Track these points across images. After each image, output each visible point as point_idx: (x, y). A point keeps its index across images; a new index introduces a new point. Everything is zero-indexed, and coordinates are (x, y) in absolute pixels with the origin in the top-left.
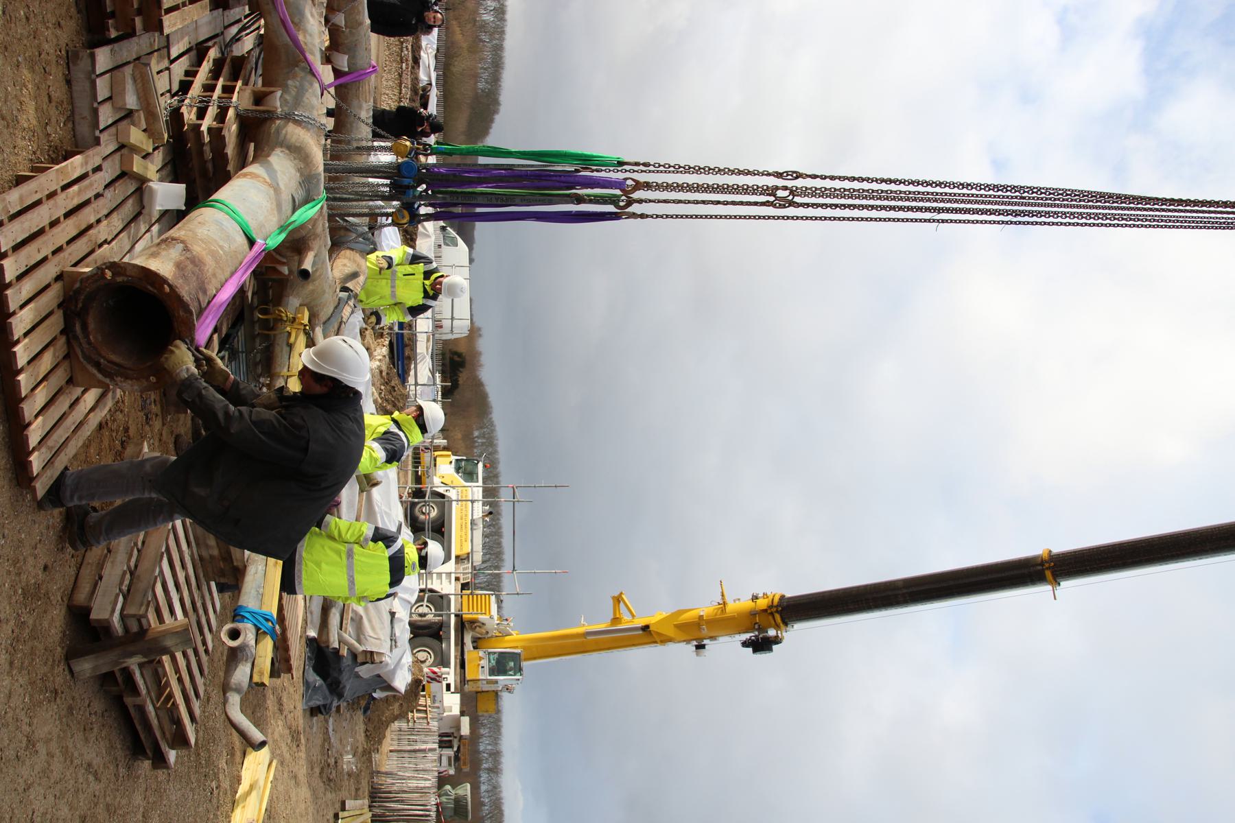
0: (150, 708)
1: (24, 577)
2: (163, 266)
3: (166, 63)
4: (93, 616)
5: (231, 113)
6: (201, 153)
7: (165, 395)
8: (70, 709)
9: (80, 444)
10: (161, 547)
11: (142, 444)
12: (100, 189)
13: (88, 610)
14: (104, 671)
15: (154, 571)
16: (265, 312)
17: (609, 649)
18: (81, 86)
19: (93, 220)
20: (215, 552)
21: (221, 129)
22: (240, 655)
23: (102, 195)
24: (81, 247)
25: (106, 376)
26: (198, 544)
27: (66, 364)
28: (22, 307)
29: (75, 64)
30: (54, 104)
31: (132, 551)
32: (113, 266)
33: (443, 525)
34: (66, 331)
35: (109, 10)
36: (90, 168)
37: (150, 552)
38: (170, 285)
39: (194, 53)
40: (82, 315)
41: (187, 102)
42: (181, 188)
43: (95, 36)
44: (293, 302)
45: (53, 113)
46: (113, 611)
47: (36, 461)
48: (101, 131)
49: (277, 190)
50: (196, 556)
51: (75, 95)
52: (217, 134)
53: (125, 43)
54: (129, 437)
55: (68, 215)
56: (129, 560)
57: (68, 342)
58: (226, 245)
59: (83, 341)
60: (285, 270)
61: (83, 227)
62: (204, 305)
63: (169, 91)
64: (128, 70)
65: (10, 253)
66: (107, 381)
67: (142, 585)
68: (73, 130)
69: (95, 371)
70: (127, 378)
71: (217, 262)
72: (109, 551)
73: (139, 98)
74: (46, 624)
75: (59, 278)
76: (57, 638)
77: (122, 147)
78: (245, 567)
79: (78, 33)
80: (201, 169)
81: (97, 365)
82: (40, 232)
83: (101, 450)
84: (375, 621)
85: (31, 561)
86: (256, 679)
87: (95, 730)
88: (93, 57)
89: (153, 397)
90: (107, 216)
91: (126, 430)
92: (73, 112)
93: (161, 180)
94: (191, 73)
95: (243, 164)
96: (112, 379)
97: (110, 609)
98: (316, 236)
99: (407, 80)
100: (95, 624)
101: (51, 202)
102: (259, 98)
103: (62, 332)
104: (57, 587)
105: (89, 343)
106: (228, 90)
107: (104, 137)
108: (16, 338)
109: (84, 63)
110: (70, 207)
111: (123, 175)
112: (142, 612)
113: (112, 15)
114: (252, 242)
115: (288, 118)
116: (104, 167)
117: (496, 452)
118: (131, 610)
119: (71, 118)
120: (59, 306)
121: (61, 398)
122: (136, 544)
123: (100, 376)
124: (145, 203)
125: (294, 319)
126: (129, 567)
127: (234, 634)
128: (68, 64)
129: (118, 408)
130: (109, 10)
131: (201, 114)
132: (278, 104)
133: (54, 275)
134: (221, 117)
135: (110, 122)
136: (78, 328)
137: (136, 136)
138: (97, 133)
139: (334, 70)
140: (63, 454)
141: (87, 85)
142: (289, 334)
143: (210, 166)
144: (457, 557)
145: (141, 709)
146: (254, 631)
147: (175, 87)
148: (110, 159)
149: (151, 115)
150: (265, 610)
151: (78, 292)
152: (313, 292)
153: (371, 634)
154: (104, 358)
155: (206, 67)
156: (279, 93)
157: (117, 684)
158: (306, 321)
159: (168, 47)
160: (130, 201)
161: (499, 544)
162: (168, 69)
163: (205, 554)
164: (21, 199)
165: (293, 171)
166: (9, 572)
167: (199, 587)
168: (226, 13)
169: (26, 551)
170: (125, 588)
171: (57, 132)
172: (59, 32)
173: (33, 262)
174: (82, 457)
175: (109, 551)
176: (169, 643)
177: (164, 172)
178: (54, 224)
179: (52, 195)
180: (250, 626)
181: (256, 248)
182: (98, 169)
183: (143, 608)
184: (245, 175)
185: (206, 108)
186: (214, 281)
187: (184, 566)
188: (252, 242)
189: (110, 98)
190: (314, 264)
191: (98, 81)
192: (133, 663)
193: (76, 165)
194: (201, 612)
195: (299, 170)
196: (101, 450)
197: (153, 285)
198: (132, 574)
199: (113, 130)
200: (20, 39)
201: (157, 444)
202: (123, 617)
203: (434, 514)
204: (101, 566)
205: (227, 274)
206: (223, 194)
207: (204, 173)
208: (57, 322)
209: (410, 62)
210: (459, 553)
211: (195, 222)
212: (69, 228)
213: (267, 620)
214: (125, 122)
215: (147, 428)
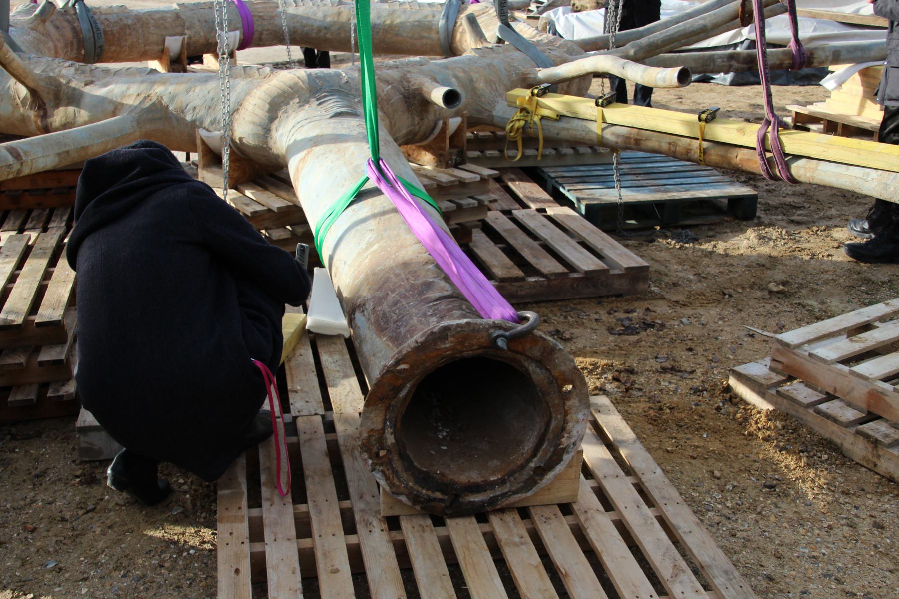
7: (619, 295)
25: (560, 460)
38: (397, 363)
44: (500, 110)
49: (316, 141)
59: (498, 491)
60: (454, 123)
62: (448, 290)
66: (567, 458)
69: (551, 475)
70: (563, 429)
75: (393, 523)
81: (541, 471)
89: (622, 315)
96: (565, 450)
98: (404, 79)
102: (213, 158)
105: (502, 482)
120: (438, 522)
121: (592, 535)
123: (559, 468)
125: (523, 110)
136: (477, 498)
142: (543, 118)
151: (415, 499)
154: (529, 461)
156: (202, 133)
158: (528, 92)
188: (360, 195)
197: (397, 390)
201: (689, 311)
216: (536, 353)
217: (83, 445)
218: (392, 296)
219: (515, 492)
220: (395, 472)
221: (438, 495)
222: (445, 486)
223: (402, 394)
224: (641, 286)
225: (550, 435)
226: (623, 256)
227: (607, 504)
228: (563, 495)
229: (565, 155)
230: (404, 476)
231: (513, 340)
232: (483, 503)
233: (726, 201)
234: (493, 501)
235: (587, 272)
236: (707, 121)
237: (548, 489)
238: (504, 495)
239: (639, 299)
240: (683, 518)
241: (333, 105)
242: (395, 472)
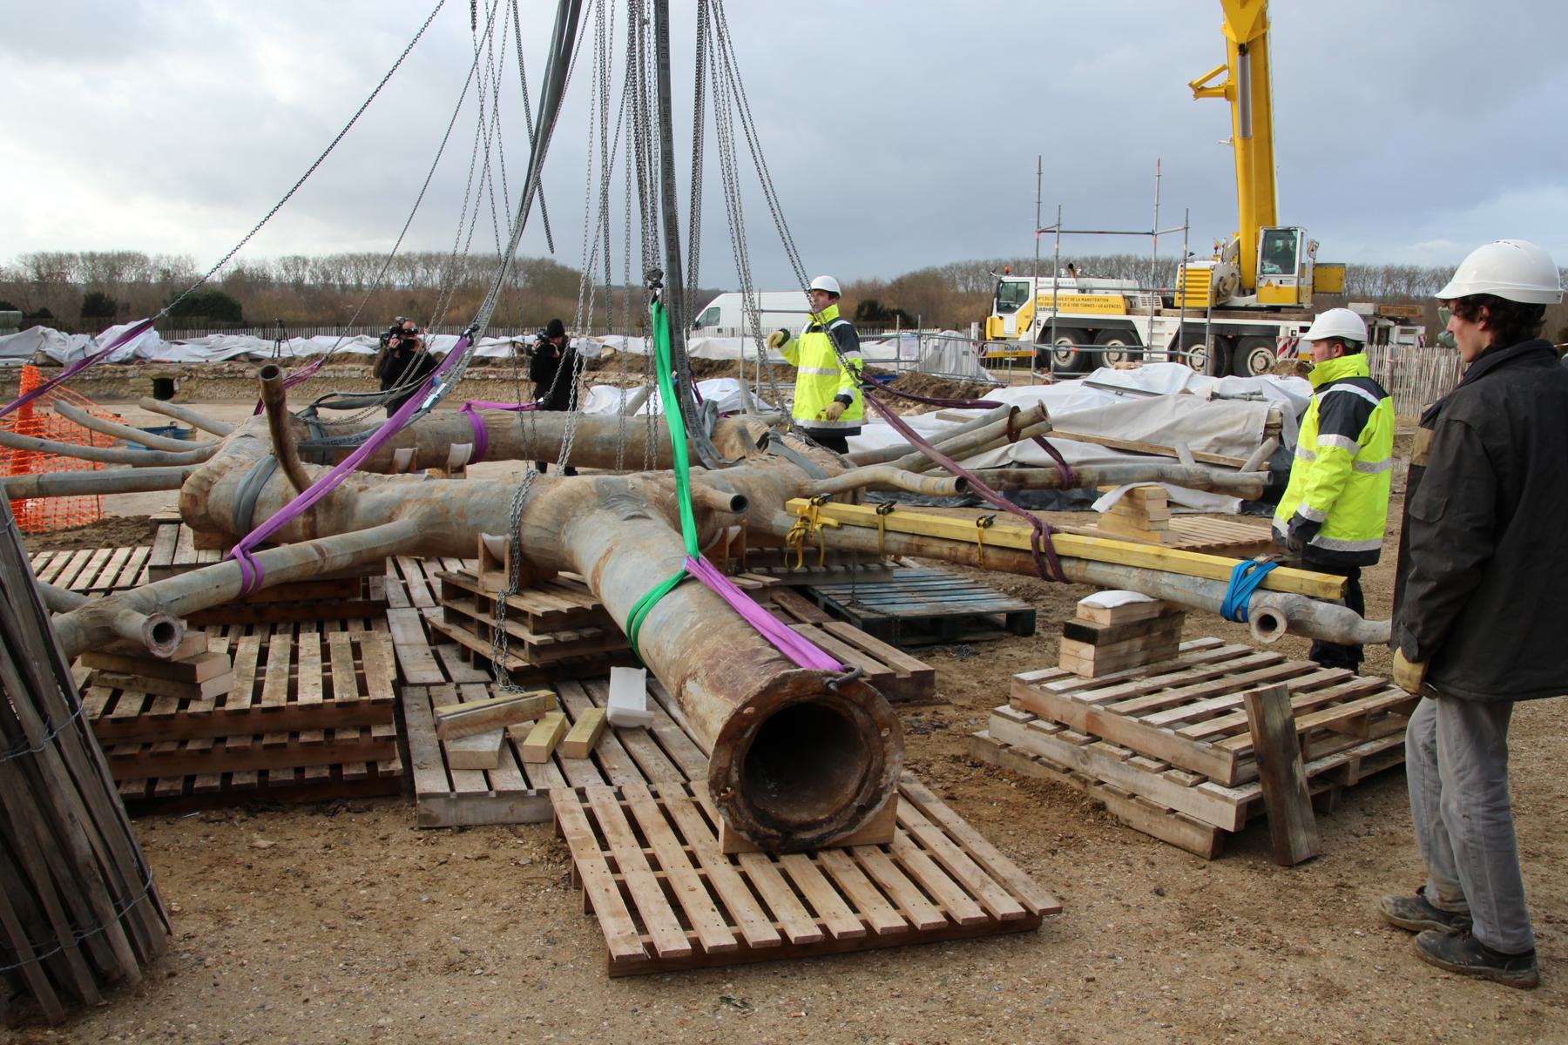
0: (1366, 749)
1: (1171, 927)
2: (712, 711)
3: (451, 687)
4: (1230, 826)
5: (515, 602)
6: (569, 644)
7: (906, 701)
8: (1363, 864)
9: (977, 836)
10: (1131, 724)
11: (977, 738)
12: (610, 791)
13: (1220, 834)
14: (1311, 815)
15: (1167, 736)
16: (793, 558)
17: (1268, 104)
18: (467, 813)
19: (652, 804)
20: (1138, 642)
21: (535, 617)
22: (1298, 617)
23: (620, 788)
24: (691, 823)
26: (1125, 667)
27: (861, 853)
28: (772, 918)
29: (437, 819)
30: (491, 852)
31: (1134, 764)
32: (715, 785)
33: (1085, 330)
34: (811, 851)
35: (365, 771)
36: (578, 807)
37: (1136, 738)
38: (745, 706)
39: (443, 651)
40: (788, 830)
41: (500, 660)
42: (616, 673)
43: (399, 789)
45: (502, 853)
46: (1225, 799)
47: (1005, 906)
48: (529, 786)
50: (1143, 670)
51: (480, 821)
52: (543, 623)
53: (414, 748)
54: (967, 756)
55: (643, 841)
56: (1148, 769)
57: (829, 849)
58: (691, 617)
59: (826, 829)
60: (734, 530)
61: (662, 819)
62: (778, 655)
63: (488, 684)
64: (451, 747)
65: (693, 934)
66: (885, 797)
67: (1187, 753)
68: (528, 824)
69: (871, 814)
70: (882, 770)
71: (715, 631)
72: (1133, 796)
73: (487, 732)
74: (1239, 896)
75: (733, 860)
76: (1261, 879)
77: (555, 757)
78: (1161, 600)
79: (397, 812)
80: (590, 648)
81: (863, 810)
82: (666, 885)
83: (984, 799)
84: (1222, 421)
85: (1146, 915)
86: (1335, 595)
87: (1393, 828)
88: (426, 797)
89: (910, 718)
90: (648, 781)
91: (956, 759)
92: (503, 825)
93: (606, 698)
94: (465, 654)
95: (579, 587)
96: (883, 790)
97: (1221, 803)
99: (508, 372)
100: (1242, 825)
101: (623, 867)
102: (494, 564)
103: (813, 856)
104: (1184, 876)
105: (830, 820)
106: (485, 604)
107: (538, 784)
108: (818, 932)
109: (436, 808)
110: (632, 838)
111: (594, 756)
112: (1230, 758)
113: (372, 765)
114: (684, 580)
115: (517, 528)
116: (577, 783)
117: (986, 264)
118: (1226, 772)
119: (512, 827)
120: (774, 859)
122: (1125, 758)
123: (879, 807)
124: (636, 724)
125: (803, 519)
126: (1158, 771)
127: (1267, 623)
128: (438, 829)
129: (920, 769)
130: (365, 771)
131: (516, 642)
132: (499, 538)
133: (729, 866)
134: (516, 615)
135: (518, 773)
136: (807, 835)
137: (538, 737)
138: (532, 793)
139: (473, 461)
140: (993, 865)
141: (464, 804)
142: (824, 526)
143: (587, 632)
144: (1128, 313)
145: (1365, 760)
146: (1260, 594)
147: (483, 675)
148: (569, 776)
149: (513, 714)
150: (1229, 576)
151: (754, 835)
152: (765, 492)
153: (1240, 427)
154: (852, 800)
155: (457, 633)
156: (486, 537)
157: (1327, 793)
158: (806, 503)
159: (428, 685)
160: (632, 746)
161: (1107, 261)
162: (458, 686)
163: (1140, 657)
164: (614, 914)
165: (593, 518)
166: (1166, 951)
167: (1187, 668)
168: (393, 604)
169: (1132, 920)
170: (1191, 779)
171: (529, 848)
172: (394, 839)
173: (709, 900)
174: (995, 828)
175: (1133, 796)
176: (1276, 721)
177: (597, 695)
178: (655, 864)
179: (614, 866)
180: (1253, 600)
181: (694, 571)
182: (581, 794)
183: (1224, 754)
184: (596, 586)
185: (509, 636)
186: (741, 638)
187: (1157, 690)
188: (684, 580)
189: (486, 773)
190: (726, 490)
191: (459, 789)
192: (1303, 771)
193: (574, 824)
194: (1223, 666)
195: (591, 511)
196: (984, 799)
197: (743, 731)
198: (1169, 767)
199: (529, 769)
200: (399, 898)
201: (975, 714)
202: (1235, 784)
203: (1068, 342)
204: (1154, 810)
205: (731, 616)
206: (620, 617)
207: (594, 640)
208: (798, 866)
209: (488, 369)
210: (1123, 310)
211: (657, 660)
212: (662, 841)
213: (1246, 573)
214: (521, 751)
215: (953, 727)
216: (861, 699)
217: (423, 812)
218: (723, 663)
219: (840, 831)
220: (738, 809)
221: (774, 832)
222: (780, 825)
223: (747, 735)
224: (926, 691)
225: (871, 776)
226: (908, 664)
227: (921, 845)
228: (880, 835)
229: (836, 573)
230: (746, 812)
231: (841, 685)
232: (812, 840)
233: (1003, 618)
234: (821, 838)
235: (874, 676)
236: (985, 526)
237: (868, 828)
238: (831, 833)
239: (925, 704)
240: (986, 851)
241: (628, 508)
242: (738, 809)
